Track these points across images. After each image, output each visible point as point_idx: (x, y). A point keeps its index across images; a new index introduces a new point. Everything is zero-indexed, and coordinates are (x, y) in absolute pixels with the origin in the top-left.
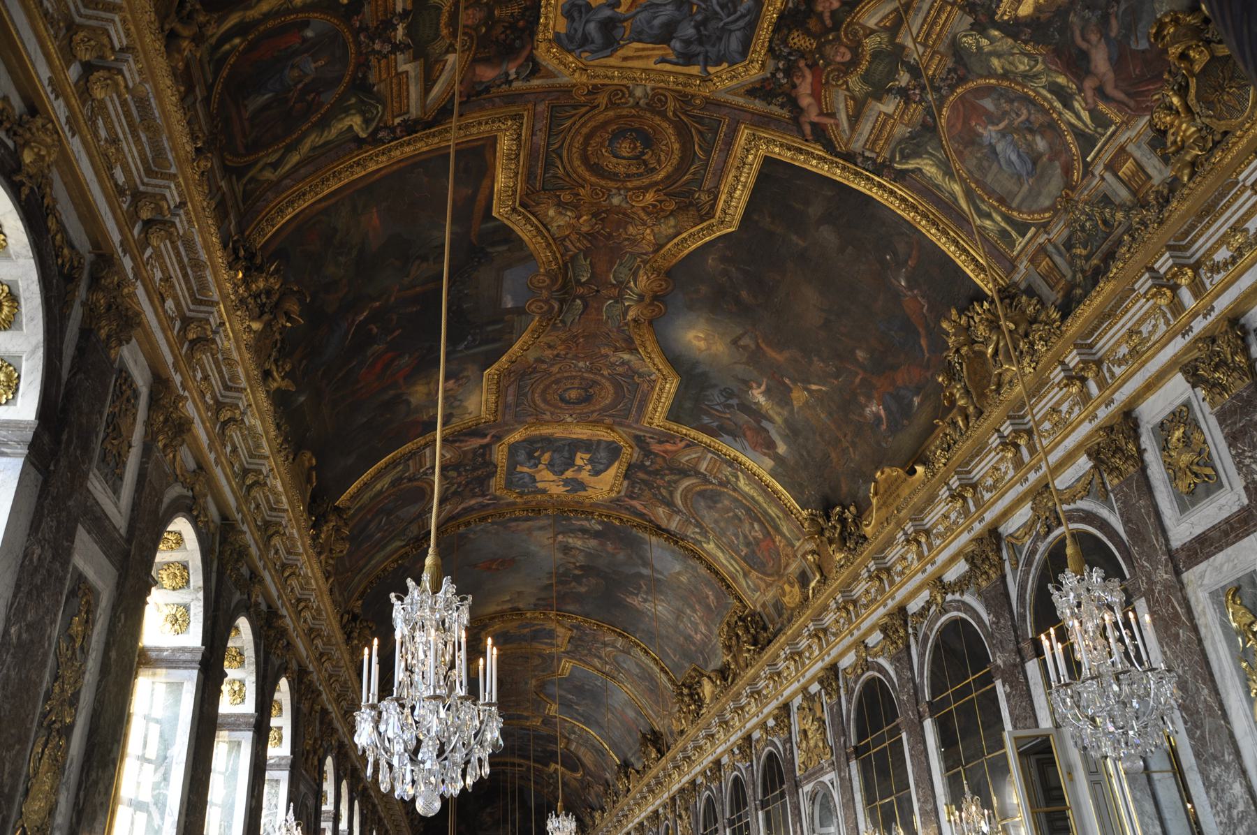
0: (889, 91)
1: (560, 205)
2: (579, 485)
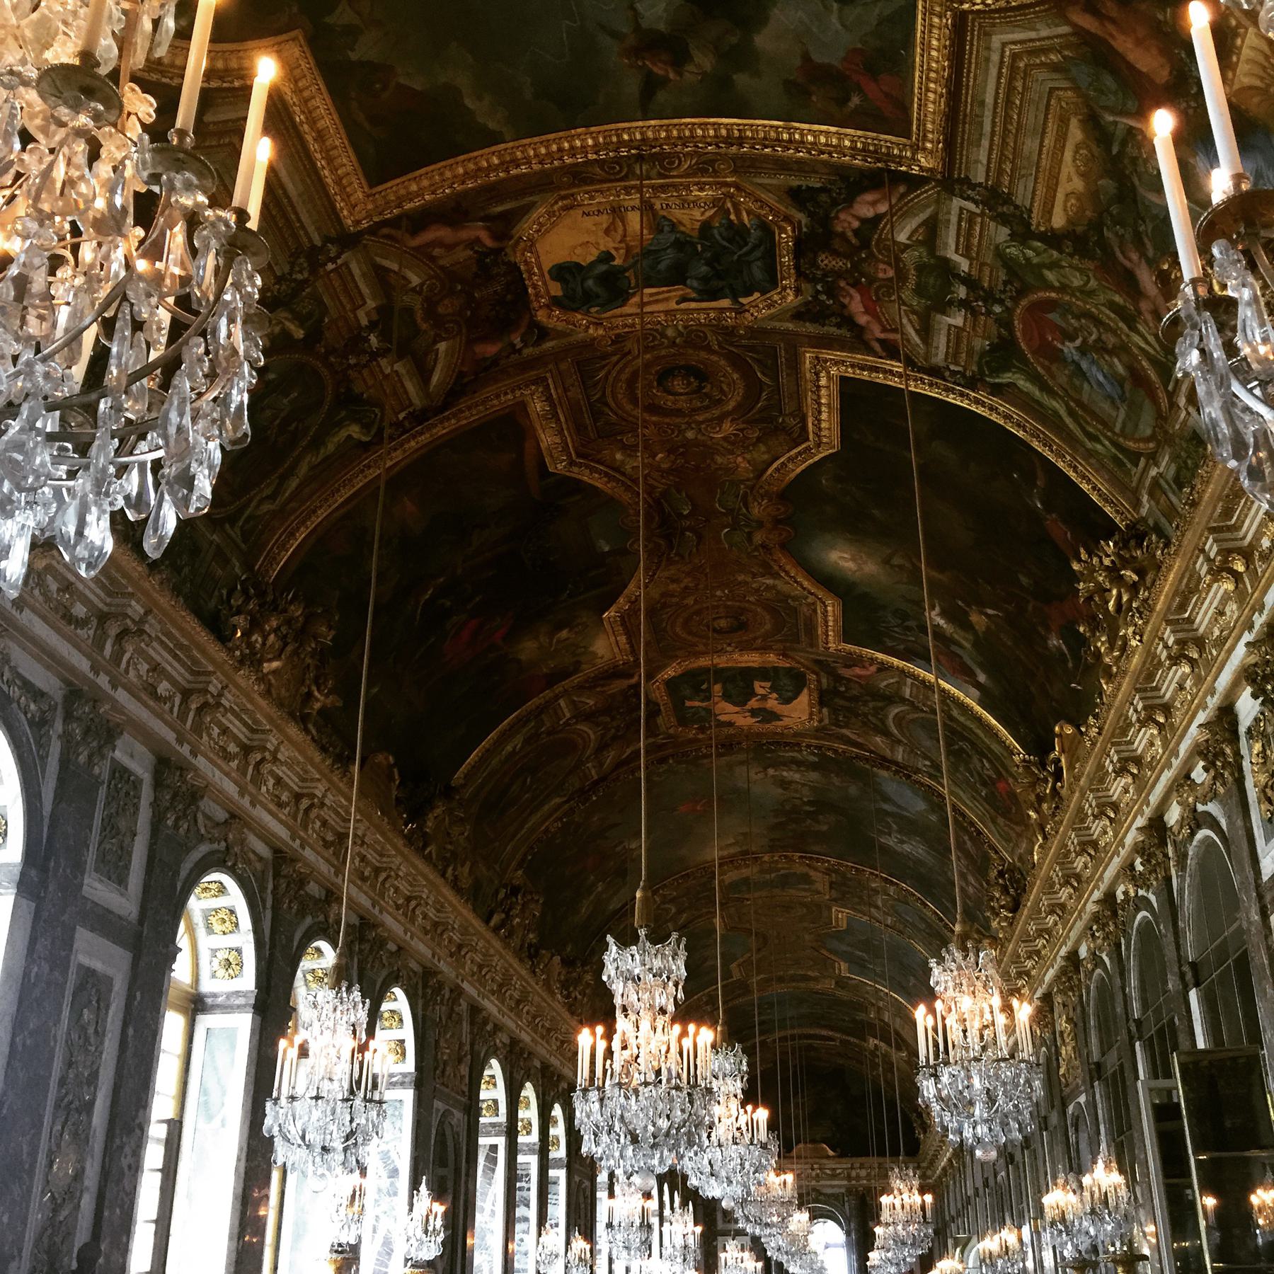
0: (951, 303)
2: (771, 716)
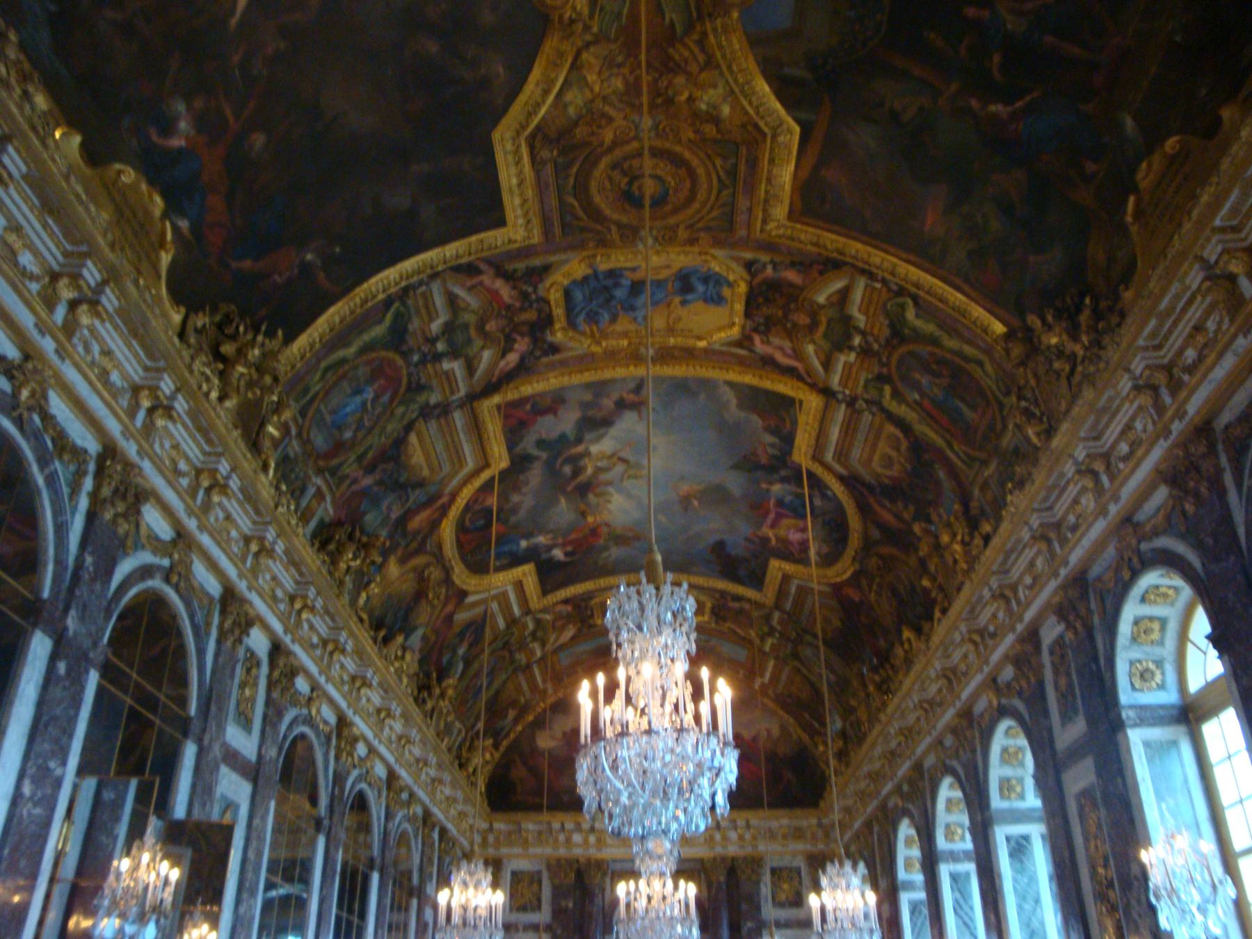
0: (443, 333)
1: (716, 120)
